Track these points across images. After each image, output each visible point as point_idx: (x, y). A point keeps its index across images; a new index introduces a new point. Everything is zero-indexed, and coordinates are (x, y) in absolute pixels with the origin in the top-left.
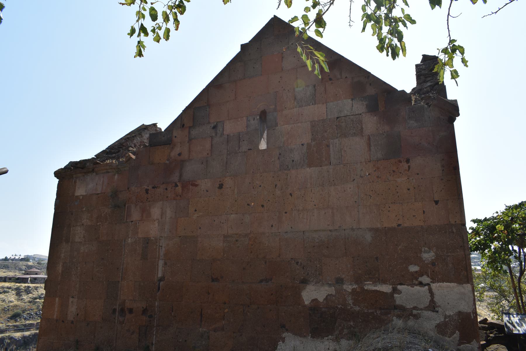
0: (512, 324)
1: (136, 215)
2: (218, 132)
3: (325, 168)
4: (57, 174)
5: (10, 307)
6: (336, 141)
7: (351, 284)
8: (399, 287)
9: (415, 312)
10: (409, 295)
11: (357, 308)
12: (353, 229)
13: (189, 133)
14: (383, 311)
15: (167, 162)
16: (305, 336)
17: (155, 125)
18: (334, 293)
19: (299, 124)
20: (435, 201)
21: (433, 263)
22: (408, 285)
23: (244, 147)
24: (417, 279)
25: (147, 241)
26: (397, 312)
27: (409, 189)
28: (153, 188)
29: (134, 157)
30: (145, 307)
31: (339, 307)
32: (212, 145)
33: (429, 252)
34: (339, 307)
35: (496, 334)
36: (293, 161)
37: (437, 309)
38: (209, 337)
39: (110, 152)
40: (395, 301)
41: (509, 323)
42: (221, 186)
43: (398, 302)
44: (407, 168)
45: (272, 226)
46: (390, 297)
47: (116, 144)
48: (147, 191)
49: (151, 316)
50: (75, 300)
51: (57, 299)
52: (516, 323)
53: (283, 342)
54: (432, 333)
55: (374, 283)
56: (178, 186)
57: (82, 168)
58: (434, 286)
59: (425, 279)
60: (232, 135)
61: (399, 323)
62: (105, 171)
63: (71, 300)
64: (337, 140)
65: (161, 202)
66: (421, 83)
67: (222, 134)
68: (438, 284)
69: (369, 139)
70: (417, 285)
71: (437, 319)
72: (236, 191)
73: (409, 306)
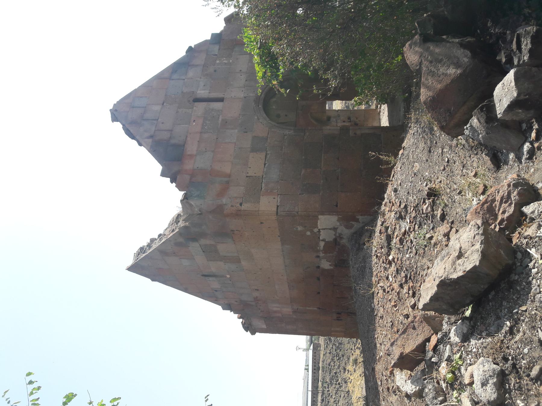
4: (253, 333)
8: (321, 238)
11: (336, 253)
12: (283, 251)
21: (305, 227)
25: (295, 312)
26: (338, 240)
43: (332, 240)
46: (327, 243)
54: (352, 231)
70: (319, 234)
73: (334, 237)
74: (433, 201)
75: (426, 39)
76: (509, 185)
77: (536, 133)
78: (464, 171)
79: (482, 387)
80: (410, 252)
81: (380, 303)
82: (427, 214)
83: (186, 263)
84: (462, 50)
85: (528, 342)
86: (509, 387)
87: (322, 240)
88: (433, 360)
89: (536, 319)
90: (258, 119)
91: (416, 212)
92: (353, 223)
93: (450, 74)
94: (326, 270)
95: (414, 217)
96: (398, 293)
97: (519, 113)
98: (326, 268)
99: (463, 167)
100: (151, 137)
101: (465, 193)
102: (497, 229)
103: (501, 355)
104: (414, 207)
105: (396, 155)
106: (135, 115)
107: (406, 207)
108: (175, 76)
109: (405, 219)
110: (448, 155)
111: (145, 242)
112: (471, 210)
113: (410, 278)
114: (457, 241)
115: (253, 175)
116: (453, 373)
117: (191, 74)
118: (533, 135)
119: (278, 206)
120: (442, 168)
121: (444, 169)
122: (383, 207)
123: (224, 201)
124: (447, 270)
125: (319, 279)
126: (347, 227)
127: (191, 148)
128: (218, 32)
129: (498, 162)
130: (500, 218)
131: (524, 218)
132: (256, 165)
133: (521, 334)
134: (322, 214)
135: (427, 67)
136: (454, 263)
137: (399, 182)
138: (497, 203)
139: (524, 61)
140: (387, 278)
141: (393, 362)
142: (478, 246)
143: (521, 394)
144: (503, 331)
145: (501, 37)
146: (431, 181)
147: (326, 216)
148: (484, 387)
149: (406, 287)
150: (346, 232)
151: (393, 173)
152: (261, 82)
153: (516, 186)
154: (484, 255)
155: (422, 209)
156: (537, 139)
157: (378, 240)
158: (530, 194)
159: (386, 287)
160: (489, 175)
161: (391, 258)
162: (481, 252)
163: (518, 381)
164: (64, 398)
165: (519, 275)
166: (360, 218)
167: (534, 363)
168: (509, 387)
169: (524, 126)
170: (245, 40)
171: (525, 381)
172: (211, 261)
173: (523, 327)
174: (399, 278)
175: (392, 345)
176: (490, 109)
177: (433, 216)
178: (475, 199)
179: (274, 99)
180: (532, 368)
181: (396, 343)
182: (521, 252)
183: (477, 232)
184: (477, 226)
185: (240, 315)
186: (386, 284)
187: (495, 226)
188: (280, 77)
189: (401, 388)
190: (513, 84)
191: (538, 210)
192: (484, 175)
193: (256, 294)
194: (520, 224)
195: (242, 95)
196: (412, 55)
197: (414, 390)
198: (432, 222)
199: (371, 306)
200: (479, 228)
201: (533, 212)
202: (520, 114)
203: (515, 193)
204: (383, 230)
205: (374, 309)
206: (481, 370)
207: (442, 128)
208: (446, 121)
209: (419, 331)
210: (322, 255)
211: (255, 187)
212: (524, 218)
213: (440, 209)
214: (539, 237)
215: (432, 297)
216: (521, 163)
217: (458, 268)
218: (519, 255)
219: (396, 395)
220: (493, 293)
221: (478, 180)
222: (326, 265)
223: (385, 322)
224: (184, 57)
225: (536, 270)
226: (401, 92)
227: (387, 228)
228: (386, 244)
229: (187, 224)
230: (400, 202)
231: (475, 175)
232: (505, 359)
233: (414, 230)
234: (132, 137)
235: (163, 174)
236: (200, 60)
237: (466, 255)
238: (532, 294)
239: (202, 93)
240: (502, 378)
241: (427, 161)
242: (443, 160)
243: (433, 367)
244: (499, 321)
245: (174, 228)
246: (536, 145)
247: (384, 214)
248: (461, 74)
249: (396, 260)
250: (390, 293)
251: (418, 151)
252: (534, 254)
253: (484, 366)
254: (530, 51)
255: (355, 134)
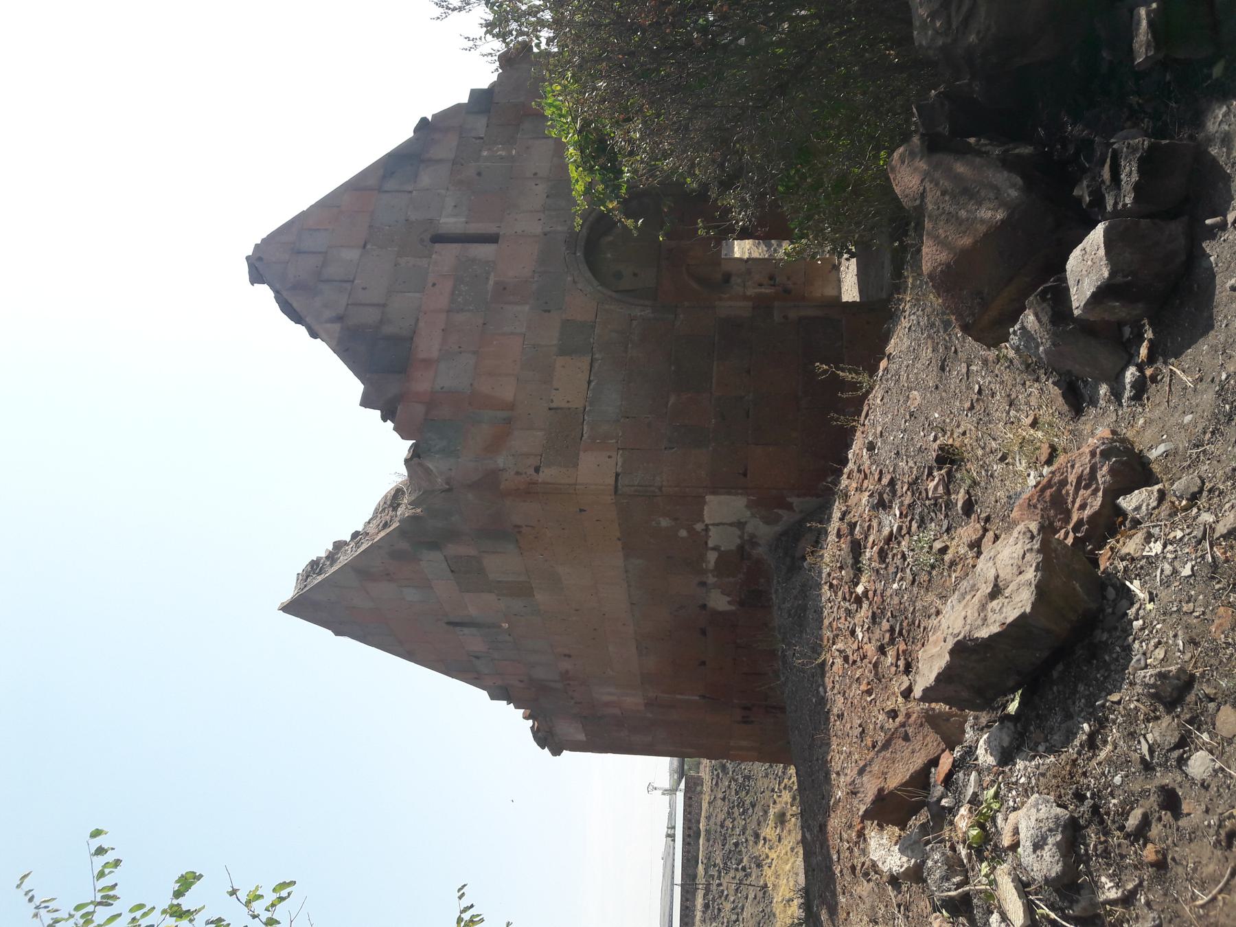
8: (710, 544)
9: (746, 537)
21: (676, 519)
25: (649, 704)
26: (747, 547)
43: (733, 548)
46: (723, 557)
54: (778, 528)
58: (707, 521)
73: (739, 541)
74: (949, 473)
75: (934, 145)
76: (1093, 454)
77: (1150, 349)
78: (1013, 413)
79: (1034, 851)
80: (902, 579)
81: (837, 686)
82: (936, 499)
83: (411, 595)
84: (1006, 174)
85: (1118, 763)
86: (1086, 851)
87: (714, 549)
88: (944, 802)
89: (1136, 718)
90: (574, 282)
91: (913, 494)
92: (780, 512)
93: (982, 221)
94: (720, 613)
95: (909, 505)
96: (876, 665)
97: (1114, 307)
98: (720, 609)
99: (1010, 405)
100: (340, 319)
101: (1014, 458)
102: (1069, 541)
103: (1069, 788)
104: (910, 484)
105: (873, 370)
106: (303, 269)
107: (892, 483)
108: (391, 185)
109: (891, 507)
110: (981, 379)
111: (321, 550)
112: (1024, 496)
113: (901, 633)
114: (991, 564)
115: (564, 405)
116: (982, 826)
117: (426, 179)
118: (1144, 351)
119: (617, 475)
120: (967, 405)
121: (972, 408)
122: (844, 481)
123: (501, 461)
124: (969, 621)
125: (704, 632)
126: (767, 522)
127: (429, 344)
128: (486, 87)
129: (1077, 399)
130: (1075, 518)
131: (1120, 519)
132: (570, 383)
133: (1109, 747)
134: (713, 493)
135: (936, 204)
136: (983, 607)
137: (879, 429)
138: (1070, 488)
139: (1125, 205)
140: (853, 633)
141: (863, 808)
142: (1030, 574)
143: (1107, 864)
144: (1077, 742)
145: (1086, 146)
146: (944, 433)
148: (1038, 852)
149: (891, 653)
150: (764, 531)
151: (865, 408)
152: (582, 204)
153: (1106, 454)
154: (1042, 591)
155: (926, 490)
156: (1151, 359)
157: (832, 550)
158: (1132, 469)
159: (849, 653)
160: (1062, 424)
161: (860, 589)
162: (1036, 586)
163: (1102, 839)
164: (177, 882)
165: (1109, 631)
166: (795, 501)
167: (1132, 803)
168: (1086, 851)
169: (1127, 331)
170: (548, 113)
171: (1116, 838)
173: (1114, 733)
174: (877, 634)
175: (861, 772)
176: (1060, 295)
177: (949, 505)
178: (1032, 473)
179: (610, 238)
180: (1128, 814)
181: (868, 769)
182: (1114, 586)
183: (1029, 546)
184: (1029, 535)
185: (528, 711)
186: (850, 646)
187: (1067, 534)
188: (623, 191)
189: (880, 865)
190: (1102, 252)
191: (1148, 505)
192: (1051, 425)
193: (566, 665)
194: (1113, 531)
195: (537, 229)
196: (908, 177)
197: (906, 866)
198: (946, 516)
199: (818, 692)
200: (1032, 537)
201: (1138, 508)
202: (1117, 310)
203: (1105, 469)
204: (845, 529)
205: (823, 698)
206: (1033, 820)
207: (966, 329)
208: (973, 315)
209: (916, 743)
210: (711, 580)
211: (567, 433)
212: (1120, 519)
213: (962, 491)
214: (1148, 557)
215: (939, 674)
216: (1121, 405)
217: (992, 617)
218: (1111, 593)
219: (868, 881)
220: (1060, 667)
221: (1040, 434)
222: (720, 602)
223: (848, 726)
224: (410, 140)
225: (1141, 622)
226: (889, 235)
227: (852, 526)
228: (850, 561)
229: (419, 510)
230: (881, 471)
231: (1034, 425)
232: (1079, 797)
233: (909, 532)
234: (296, 317)
235: (366, 402)
236: (446, 149)
237: (1007, 592)
238: (1130, 670)
239: (451, 222)
240: (1072, 833)
241: (937, 387)
242: (969, 388)
243: (944, 818)
244: (1070, 723)
245: (388, 518)
246: (1148, 372)
247: (846, 496)
248: (1002, 221)
249: (871, 594)
250: (859, 663)
251: (919, 365)
252: (1138, 592)
253: (1038, 811)
254: (1137, 188)
255: (785, 317)
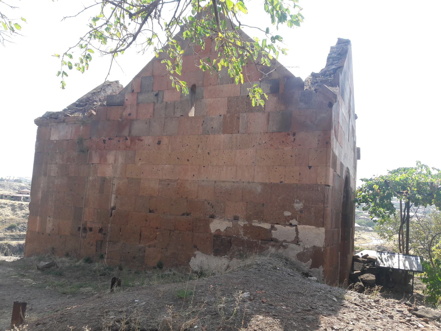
0: (381, 260)
1: (96, 159)
2: (159, 99)
3: (234, 135)
4: (38, 122)
5: (7, 220)
6: (245, 114)
7: (243, 221)
8: (276, 226)
10: (282, 232)
11: (246, 238)
12: (249, 182)
13: (137, 97)
14: (263, 241)
15: (120, 120)
16: (209, 254)
17: (117, 82)
18: (231, 226)
19: (219, 99)
20: (309, 166)
21: (301, 211)
22: (282, 225)
23: (178, 114)
24: (288, 221)
25: (104, 180)
26: (272, 243)
27: (292, 156)
28: (109, 139)
29: (94, 113)
30: (101, 227)
31: (234, 236)
32: (154, 109)
33: (300, 203)
34: (234, 236)
35: (371, 266)
36: (212, 128)
37: (299, 243)
38: (145, 251)
39: (79, 104)
40: (272, 235)
41: (380, 258)
42: (159, 143)
43: (274, 236)
44: (293, 140)
45: (194, 175)
46: (268, 232)
47: (84, 97)
48: (104, 141)
49: (105, 234)
50: (51, 219)
51: (38, 218)
52: (385, 259)
53: (195, 257)
54: (294, 259)
55: (260, 222)
56: (127, 139)
57: (56, 119)
58: (299, 227)
59: (294, 222)
60: (169, 102)
61: (272, 250)
62: (73, 122)
63: (48, 218)
64: (245, 114)
65: (115, 151)
66: (329, 65)
67: (162, 101)
68: (302, 226)
69: (269, 115)
71: (298, 249)
72: (170, 148)
73: (281, 239)
147: (324, 235)
172: (229, 101)
